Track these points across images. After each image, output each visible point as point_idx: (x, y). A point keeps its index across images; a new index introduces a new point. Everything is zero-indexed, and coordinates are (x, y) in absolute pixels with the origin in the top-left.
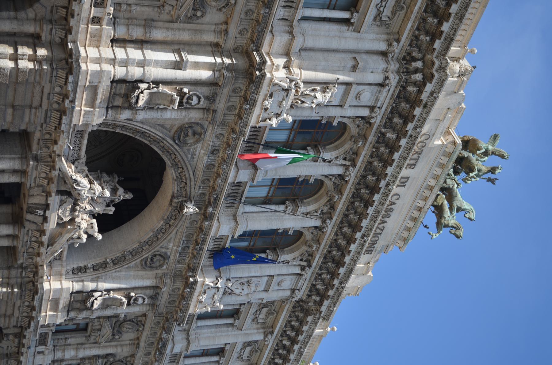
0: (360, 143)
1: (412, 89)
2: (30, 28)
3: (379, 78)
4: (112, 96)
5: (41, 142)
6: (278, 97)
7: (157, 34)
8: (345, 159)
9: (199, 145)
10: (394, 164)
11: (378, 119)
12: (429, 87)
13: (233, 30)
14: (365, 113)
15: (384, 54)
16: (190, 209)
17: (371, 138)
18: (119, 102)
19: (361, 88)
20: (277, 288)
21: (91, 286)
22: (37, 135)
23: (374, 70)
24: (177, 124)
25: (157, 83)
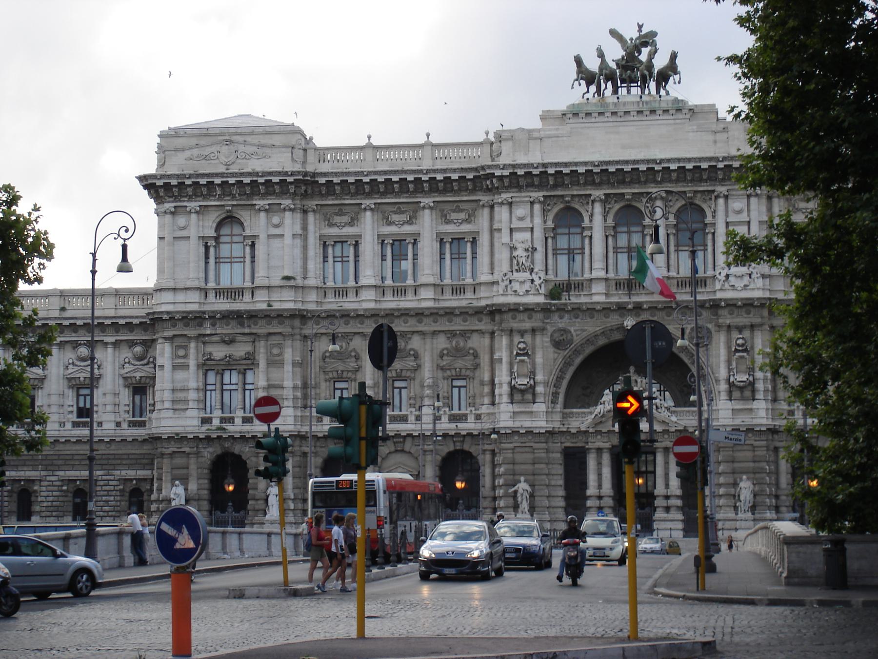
0: (567, 199)
1: (506, 182)
2: (488, 457)
3: (505, 210)
4: (523, 401)
5: (574, 441)
6: (516, 286)
7: (487, 377)
8: (588, 203)
9: (572, 329)
10: (574, 168)
11: (539, 195)
12: (498, 173)
13: (481, 326)
14: (537, 207)
15: (492, 207)
16: (629, 323)
17: (559, 193)
18: (529, 397)
19: (514, 219)
20: (745, 214)
21: (723, 386)
22: (568, 444)
23: (502, 213)
24: (551, 350)
25: (512, 373)
